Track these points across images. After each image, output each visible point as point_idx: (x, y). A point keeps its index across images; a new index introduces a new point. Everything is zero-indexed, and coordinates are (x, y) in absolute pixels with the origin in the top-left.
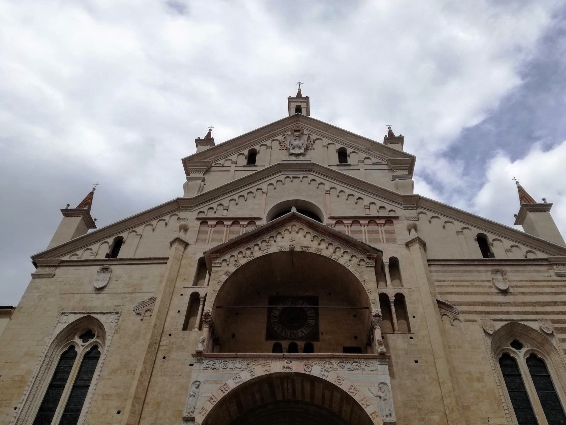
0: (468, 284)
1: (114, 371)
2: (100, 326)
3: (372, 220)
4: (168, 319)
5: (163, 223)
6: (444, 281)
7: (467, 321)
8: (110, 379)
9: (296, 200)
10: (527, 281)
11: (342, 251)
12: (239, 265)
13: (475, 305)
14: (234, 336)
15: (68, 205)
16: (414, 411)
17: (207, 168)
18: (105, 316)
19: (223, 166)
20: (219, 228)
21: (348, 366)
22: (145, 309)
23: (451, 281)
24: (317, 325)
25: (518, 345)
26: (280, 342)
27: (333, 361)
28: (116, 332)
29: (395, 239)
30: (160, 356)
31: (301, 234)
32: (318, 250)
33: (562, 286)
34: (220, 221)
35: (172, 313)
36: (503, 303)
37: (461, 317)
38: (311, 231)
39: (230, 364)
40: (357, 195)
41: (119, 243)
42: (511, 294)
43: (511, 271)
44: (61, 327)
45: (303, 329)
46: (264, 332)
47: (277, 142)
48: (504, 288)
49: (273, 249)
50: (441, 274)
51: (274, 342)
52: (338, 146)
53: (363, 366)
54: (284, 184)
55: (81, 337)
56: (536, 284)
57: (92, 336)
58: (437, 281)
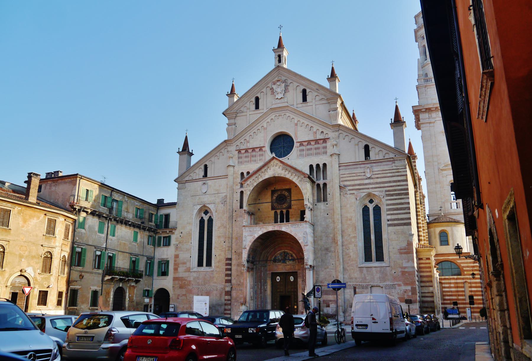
0: (354, 175)
1: (219, 228)
2: (210, 209)
3: (317, 141)
4: (234, 204)
5: (221, 154)
6: (345, 174)
7: (350, 194)
8: (219, 230)
9: (281, 132)
10: (381, 171)
11: (294, 175)
12: (254, 187)
13: (355, 186)
14: (259, 210)
15: (179, 148)
16: (324, 234)
17: (235, 116)
18: (210, 205)
19: (243, 112)
20: (246, 154)
21: (294, 226)
22: (224, 200)
23: (348, 174)
24: (291, 202)
25: (371, 201)
26: (277, 211)
27: (289, 225)
28: (216, 212)
29: (327, 152)
30: (234, 220)
31: (277, 167)
32: (285, 175)
33: (396, 172)
34: (246, 151)
35: (235, 201)
36: (367, 184)
37: (349, 192)
38: (281, 165)
39: (255, 229)
40: (310, 125)
41: (206, 167)
42: (372, 178)
43: (375, 166)
44: (196, 211)
45: (285, 204)
46: (270, 207)
47: (268, 89)
48: (369, 176)
49: (267, 177)
50: (344, 171)
51: (274, 211)
52: (302, 88)
53: (299, 226)
54: (274, 121)
55: (204, 213)
56: (384, 172)
57: (208, 212)
58: (341, 175)
